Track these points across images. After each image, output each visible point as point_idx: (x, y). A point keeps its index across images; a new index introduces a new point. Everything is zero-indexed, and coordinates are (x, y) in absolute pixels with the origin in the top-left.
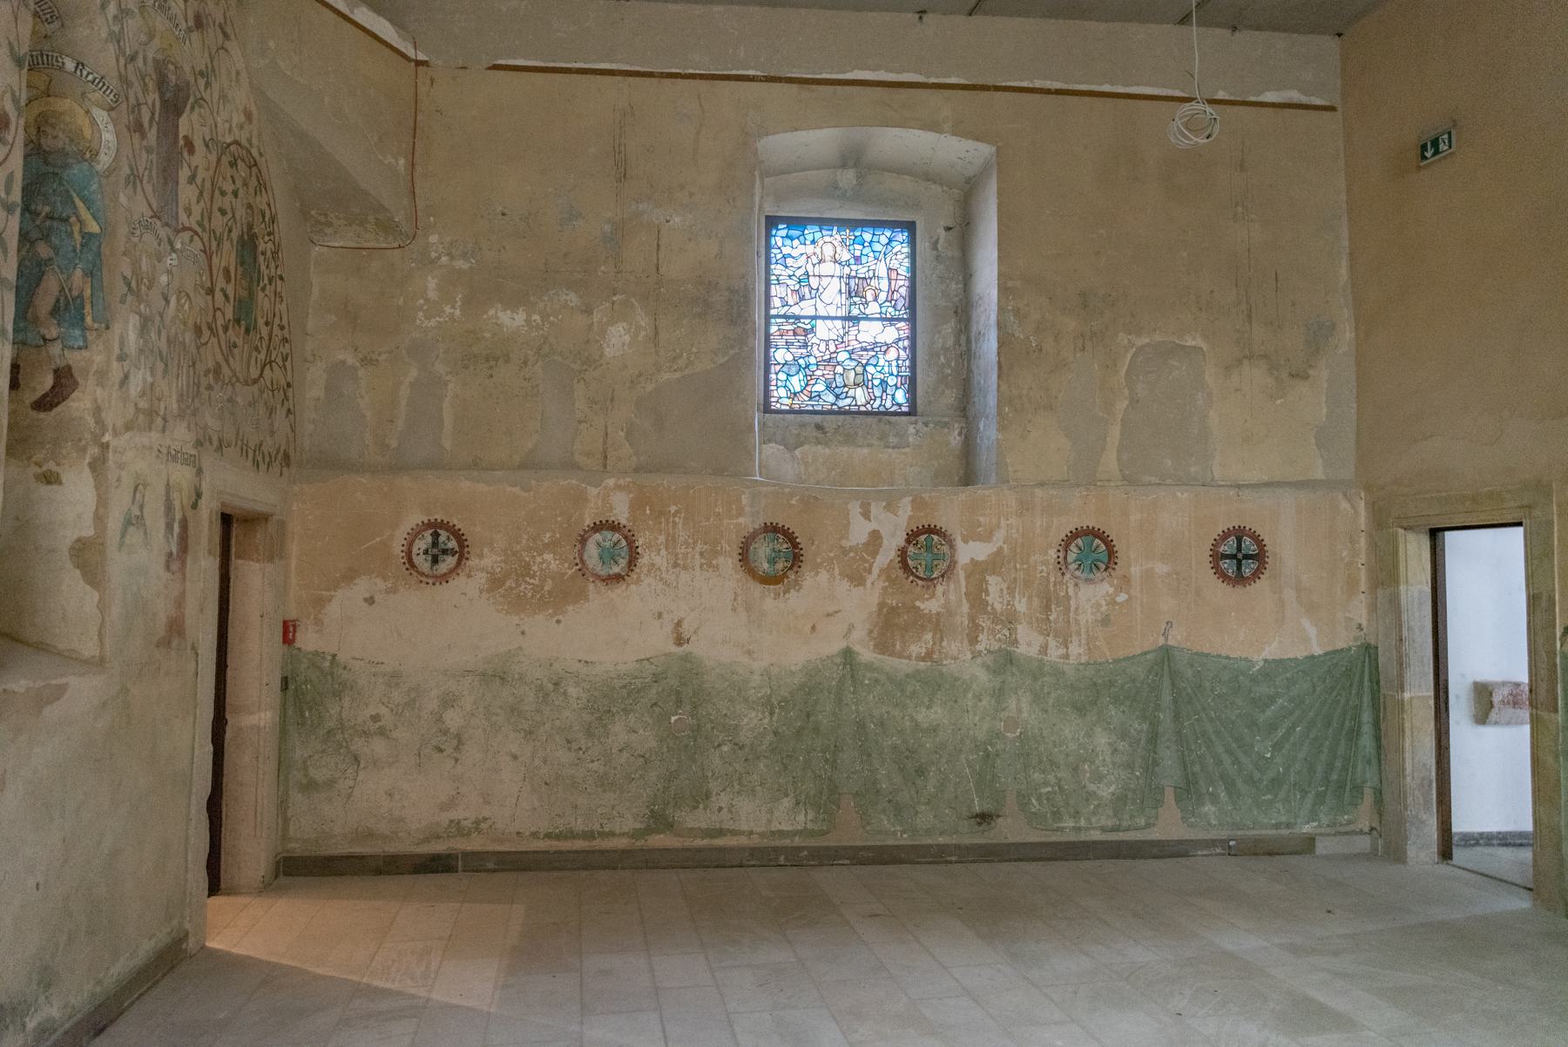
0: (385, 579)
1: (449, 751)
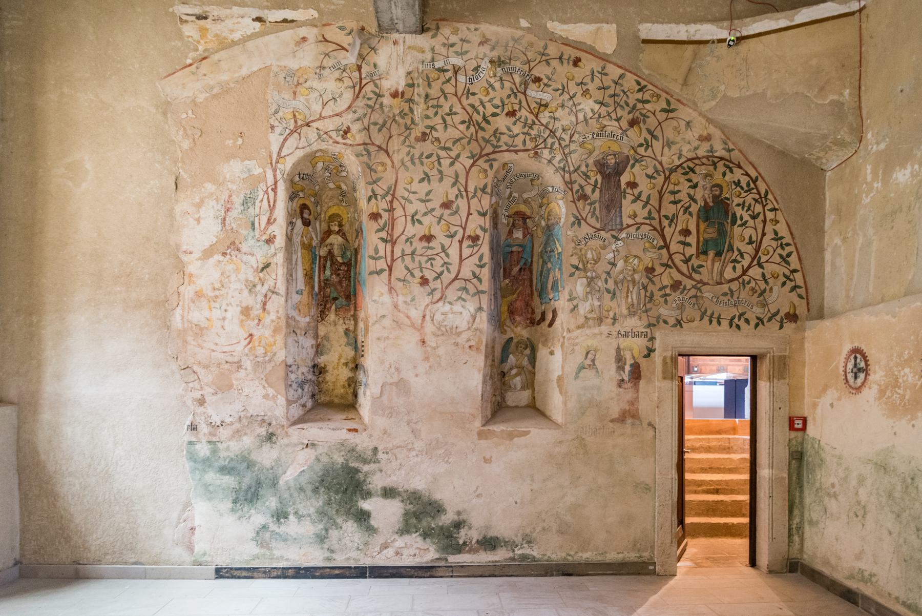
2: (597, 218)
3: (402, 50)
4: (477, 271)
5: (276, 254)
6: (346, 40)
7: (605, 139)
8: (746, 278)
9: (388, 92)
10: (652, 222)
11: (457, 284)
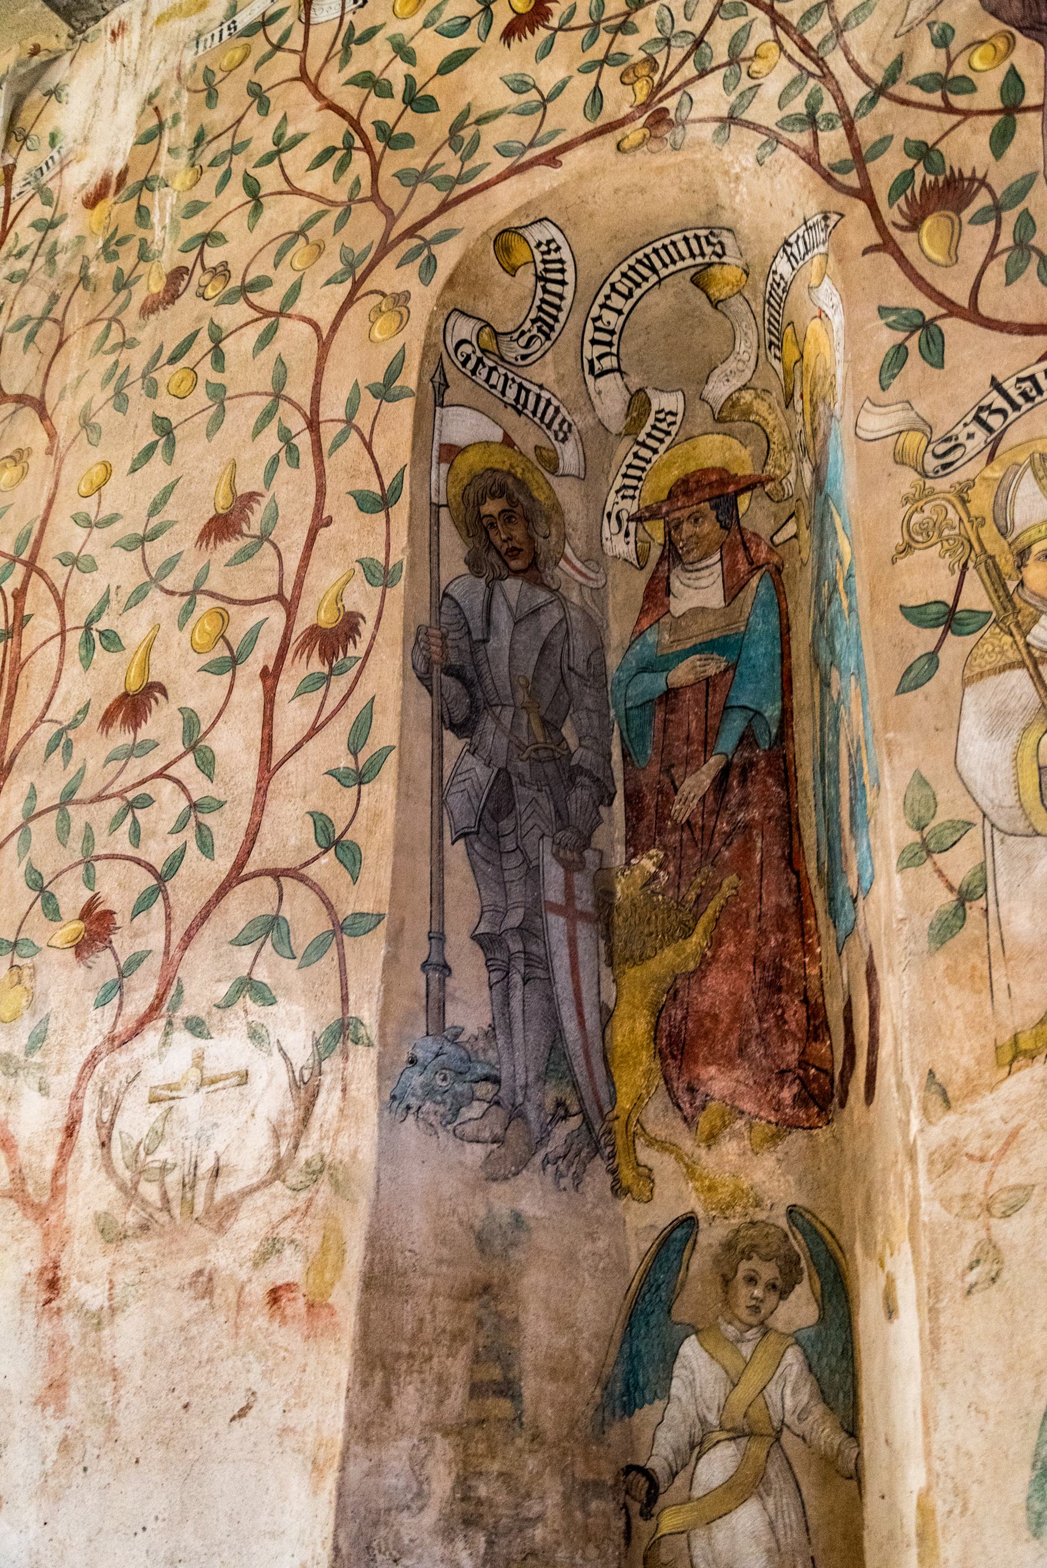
3: (135, 45)
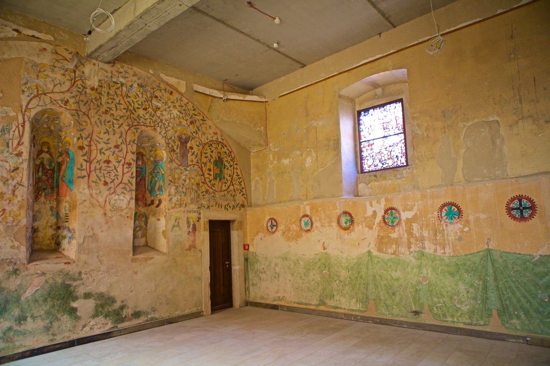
0: (263, 233)
1: (277, 278)
2: (179, 160)
3: (97, 69)
4: (131, 180)
5: (22, 163)
6: (69, 56)
7: (181, 127)
8: (229, 190)
9: (89, 87)
10: (199, 164)
11: (122, 186)
